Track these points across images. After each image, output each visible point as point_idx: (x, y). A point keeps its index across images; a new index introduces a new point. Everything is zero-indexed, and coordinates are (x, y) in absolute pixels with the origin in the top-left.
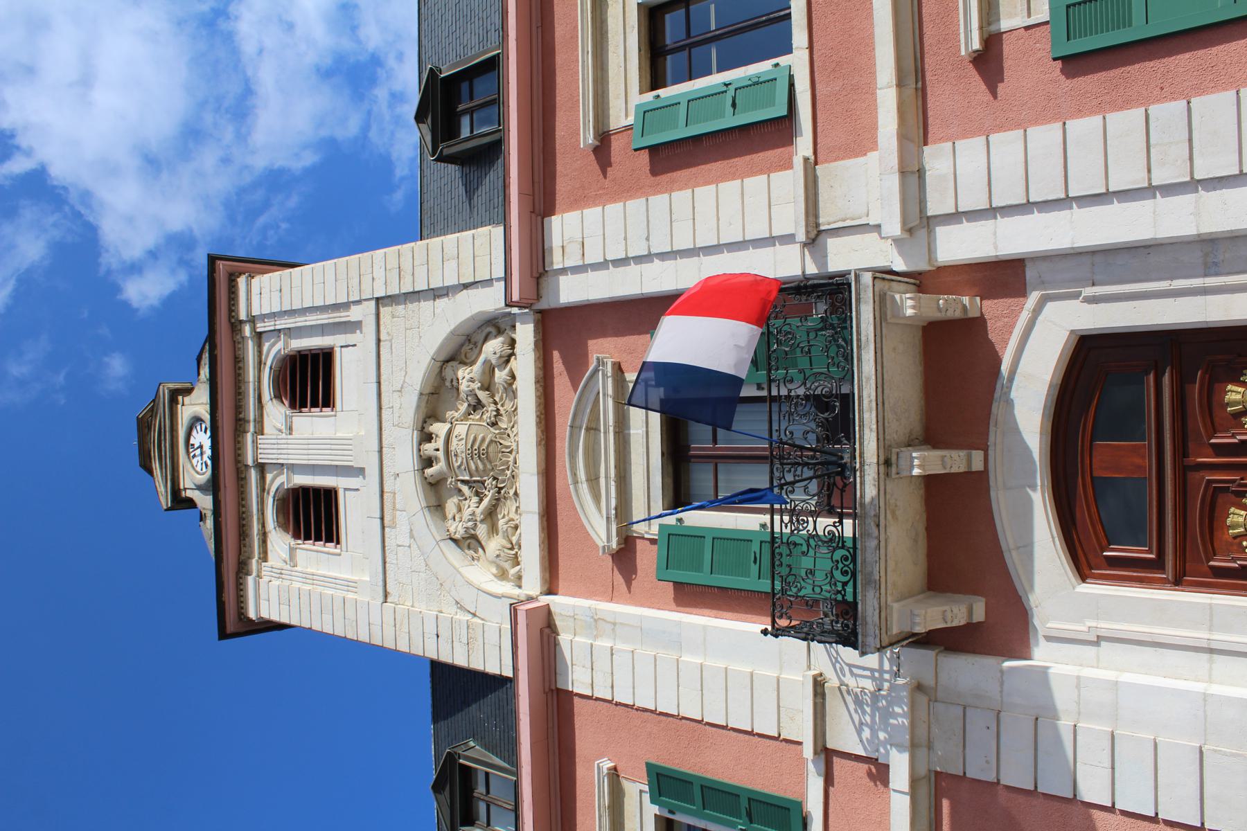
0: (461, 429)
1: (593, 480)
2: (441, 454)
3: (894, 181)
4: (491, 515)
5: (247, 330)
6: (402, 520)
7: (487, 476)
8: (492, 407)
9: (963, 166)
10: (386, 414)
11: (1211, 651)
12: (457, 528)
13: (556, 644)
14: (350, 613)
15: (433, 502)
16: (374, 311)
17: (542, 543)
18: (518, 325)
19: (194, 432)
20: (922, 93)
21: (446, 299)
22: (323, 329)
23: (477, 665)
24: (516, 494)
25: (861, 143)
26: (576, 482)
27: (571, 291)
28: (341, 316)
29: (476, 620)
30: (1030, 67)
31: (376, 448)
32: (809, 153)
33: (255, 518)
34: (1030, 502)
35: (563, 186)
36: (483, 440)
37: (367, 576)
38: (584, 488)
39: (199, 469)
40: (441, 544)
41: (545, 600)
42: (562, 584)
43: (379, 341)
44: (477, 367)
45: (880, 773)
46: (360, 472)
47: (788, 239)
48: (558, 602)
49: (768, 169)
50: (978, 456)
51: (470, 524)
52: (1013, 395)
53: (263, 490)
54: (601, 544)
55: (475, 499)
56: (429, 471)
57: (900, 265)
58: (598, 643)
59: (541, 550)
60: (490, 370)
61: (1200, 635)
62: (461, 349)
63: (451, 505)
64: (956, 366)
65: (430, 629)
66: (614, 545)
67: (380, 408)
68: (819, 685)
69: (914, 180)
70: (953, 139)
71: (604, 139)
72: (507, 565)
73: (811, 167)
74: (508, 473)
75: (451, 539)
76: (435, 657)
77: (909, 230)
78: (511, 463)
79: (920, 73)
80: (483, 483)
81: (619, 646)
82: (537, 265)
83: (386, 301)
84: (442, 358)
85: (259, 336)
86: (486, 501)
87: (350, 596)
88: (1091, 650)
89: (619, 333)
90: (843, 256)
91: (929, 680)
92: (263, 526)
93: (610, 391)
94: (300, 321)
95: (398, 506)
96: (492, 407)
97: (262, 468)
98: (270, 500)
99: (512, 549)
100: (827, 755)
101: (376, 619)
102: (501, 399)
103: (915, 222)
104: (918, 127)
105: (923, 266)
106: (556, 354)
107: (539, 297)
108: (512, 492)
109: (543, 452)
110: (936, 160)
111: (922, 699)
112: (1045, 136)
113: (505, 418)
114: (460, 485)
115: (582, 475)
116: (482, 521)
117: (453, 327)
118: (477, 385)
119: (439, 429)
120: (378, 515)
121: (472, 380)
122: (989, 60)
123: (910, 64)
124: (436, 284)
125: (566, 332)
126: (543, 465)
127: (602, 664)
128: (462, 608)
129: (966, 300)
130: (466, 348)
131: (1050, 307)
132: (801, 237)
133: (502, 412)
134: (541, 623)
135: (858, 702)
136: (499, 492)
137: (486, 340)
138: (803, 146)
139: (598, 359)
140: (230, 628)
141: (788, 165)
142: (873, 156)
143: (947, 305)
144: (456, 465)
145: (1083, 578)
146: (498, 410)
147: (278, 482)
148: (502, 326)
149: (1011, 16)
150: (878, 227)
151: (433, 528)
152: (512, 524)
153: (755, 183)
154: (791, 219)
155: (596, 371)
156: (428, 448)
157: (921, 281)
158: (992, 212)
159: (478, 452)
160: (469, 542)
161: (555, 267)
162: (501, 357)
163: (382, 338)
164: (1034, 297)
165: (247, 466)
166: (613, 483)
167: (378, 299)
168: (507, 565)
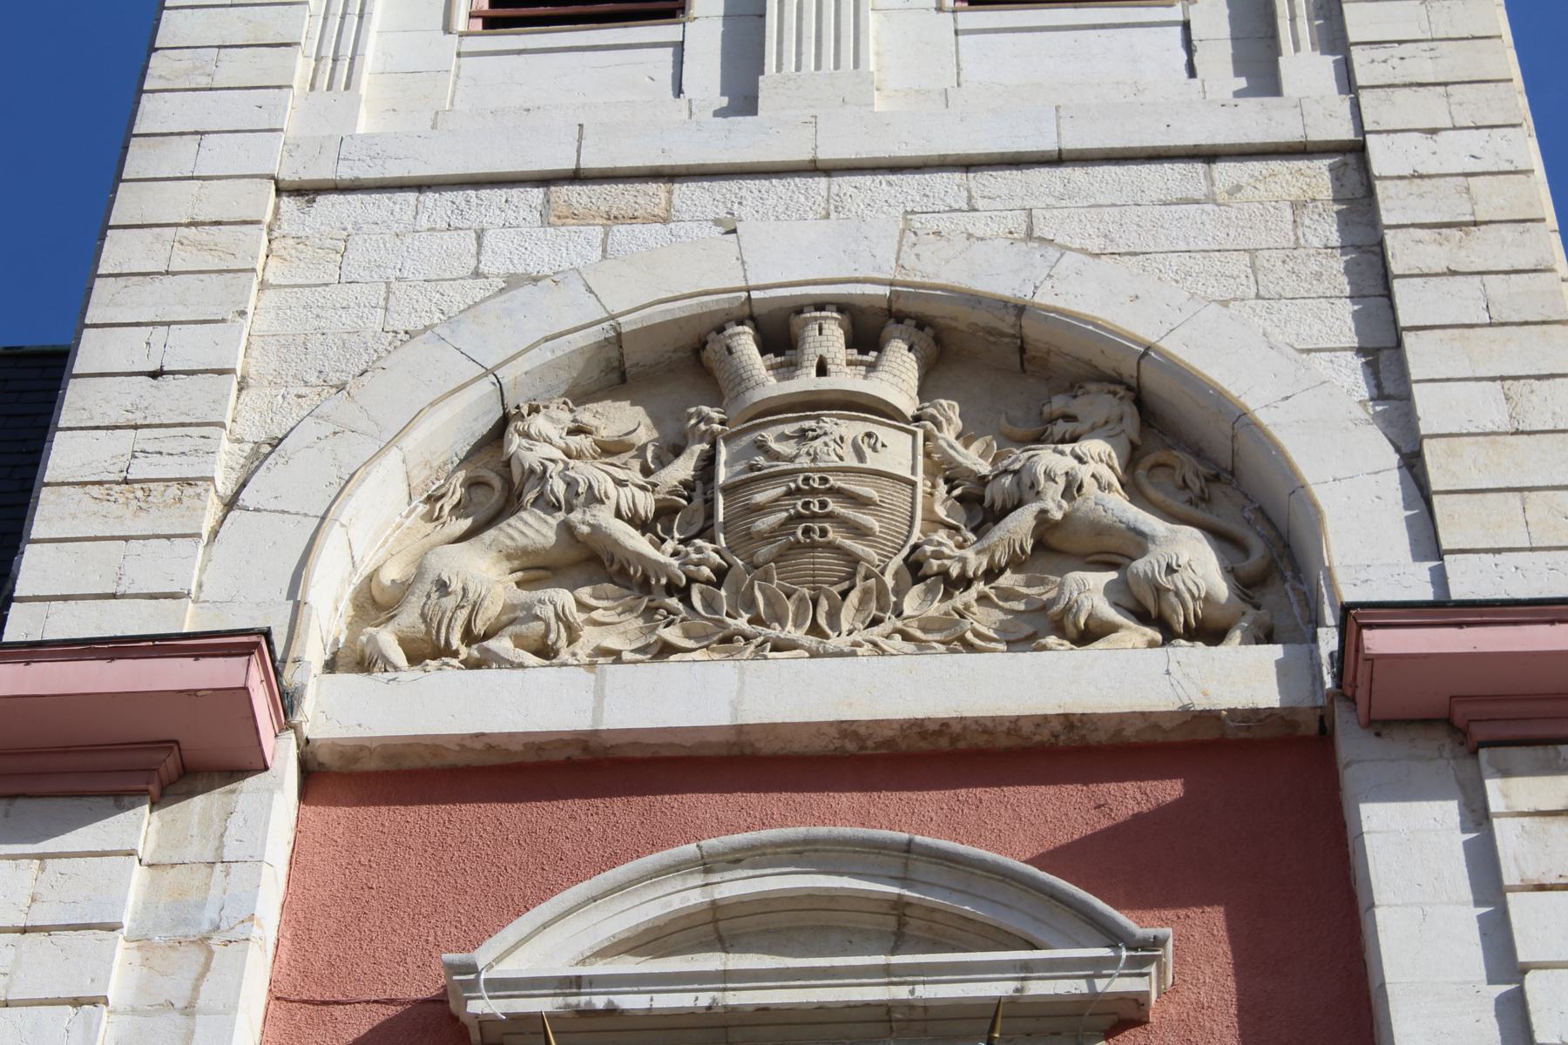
0: (896, 452)
1: (715, 927)
2: (806, 381)
4: (588, 560)
6: (575, 246)
8: (976, 562)
10: (947, 185)
12: (543, 442)
13: (120, 798)
15: (635, 356)
16: (1317, 135)
17: (488, 742)
18: (1276, 651)
21: (1364, 392)
23: (51, 514)
24: (665, 650)
26: (707, 864)
27: (1406, 845)
29: (213, 509)
36: (860, 532)
37: (375, 122)
38: (687, 895)
40: (486, 386)
41: (283, 756)
42: (338, 817)
43: (1208, 156)
44: (1119, 507)
46: (742, 97)
48: (270, 808)
51: (559, 487)
54: (482, 957)
55: (646, 504)
56: (745, 342)
58: (121, 950)
59: (464, 742)
60: (1112, 550)
62: (1189, 448)
63: (623, 418)
66: (476, 1007)
72: (409, 618)
74: (742, 623)
75: (504, 423)
78: (775, 631)
80: (706, 532)
83: (1353, 177)
84: (1152, 380)
86: (639, 543)
87: (302, 66)
93: (1039, 988)
95: (620, 232)
96: (976, 562)
99: (469, 637)
101: (218, 155)
102: (1008, 595)
106: (1170, 790)
107: (1379, 725)
108: (673, 635)
109: (818, 746)
113: (936, 608)
114: (698, 449)
115: (736, 886)
116: (567, 529)
117: (1264, 417)
118: (1054, 504)
119: (897, 376)
120: (593, 160)
121: (1072, 488)
124: (1420, 355)
126: (766, 747)
130: (1188, 466)
133: (960, 599)
136: (671, 589)
137: (1220, 537)
139: (1158, 943)
144: (769, 435)
146: (965, 582)
148: (1269, 597)
151: (545, 354)
152: (559, 636)
155: (1112, 935)
156: (829, 339)
159: (817, 509)
160: (492, 483)
161: (1493, 786)
162: (1159, 591)
166: (705, 1000)
168: (409, 618)
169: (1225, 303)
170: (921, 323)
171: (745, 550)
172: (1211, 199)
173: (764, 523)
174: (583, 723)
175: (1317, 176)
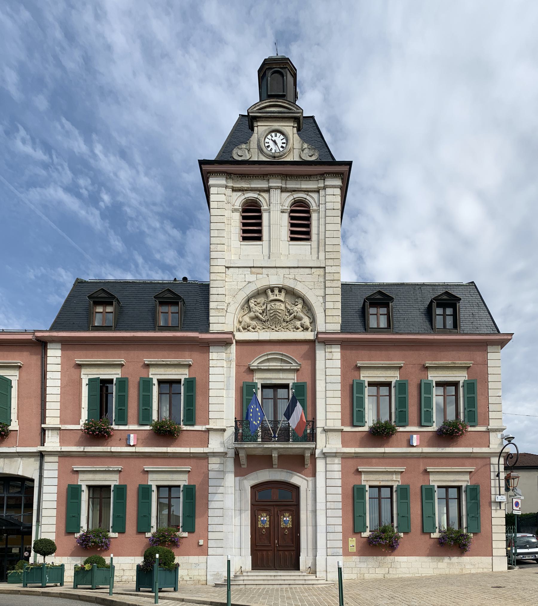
0: (282, 307)
2: (275, 298)
6: (252, 278)
9: (336, 465)
10: (287, 270)
12: (252, 305)
14: (219, 247)
15: (260, 292)
16: (321, 266)
17: (250, 340)
18: (313, 333)
25: (345, 444)
26: (267, 355)
27: (320, 354)
30: (353, 481)
32: (344, 430)
33: (249, 186)
36: (280, 316)
44: (302, 315)
53: (260, 191)
55: (261, 311)
60: (300, 319)
62: (308, 307)
65: (220, 291)
69: (334, 455)
73: (342, 431)
76: (211, 286)
77: (324, 454)
82: (327, 342)
86: (261, 316)
87: (226, 247)
92: (246, 190)
98: (256, 196)
103: (326, 455)
104: (345, 457)
105: (316, 456)
107: (319, 342)
110: (337, 460)
112: (339, 483)
118: (295, 314)
119: (282, 297)
120: (255, 266)
130: (307, 308)
132: (325, 428)
134: (228, 341)
140: (205, 167)
141: (342, 425)
142: (341, 446)
144: (272, 304)
147: (263, 199)
148: (312, 325)
153: (339, 416)
154: (331, 425)
155: (297, 363)
156: (276, 292)
157: (313, 455)
163: (313, 269)
171: (270, 320)
172: (311, 274)
174: (257, 339)
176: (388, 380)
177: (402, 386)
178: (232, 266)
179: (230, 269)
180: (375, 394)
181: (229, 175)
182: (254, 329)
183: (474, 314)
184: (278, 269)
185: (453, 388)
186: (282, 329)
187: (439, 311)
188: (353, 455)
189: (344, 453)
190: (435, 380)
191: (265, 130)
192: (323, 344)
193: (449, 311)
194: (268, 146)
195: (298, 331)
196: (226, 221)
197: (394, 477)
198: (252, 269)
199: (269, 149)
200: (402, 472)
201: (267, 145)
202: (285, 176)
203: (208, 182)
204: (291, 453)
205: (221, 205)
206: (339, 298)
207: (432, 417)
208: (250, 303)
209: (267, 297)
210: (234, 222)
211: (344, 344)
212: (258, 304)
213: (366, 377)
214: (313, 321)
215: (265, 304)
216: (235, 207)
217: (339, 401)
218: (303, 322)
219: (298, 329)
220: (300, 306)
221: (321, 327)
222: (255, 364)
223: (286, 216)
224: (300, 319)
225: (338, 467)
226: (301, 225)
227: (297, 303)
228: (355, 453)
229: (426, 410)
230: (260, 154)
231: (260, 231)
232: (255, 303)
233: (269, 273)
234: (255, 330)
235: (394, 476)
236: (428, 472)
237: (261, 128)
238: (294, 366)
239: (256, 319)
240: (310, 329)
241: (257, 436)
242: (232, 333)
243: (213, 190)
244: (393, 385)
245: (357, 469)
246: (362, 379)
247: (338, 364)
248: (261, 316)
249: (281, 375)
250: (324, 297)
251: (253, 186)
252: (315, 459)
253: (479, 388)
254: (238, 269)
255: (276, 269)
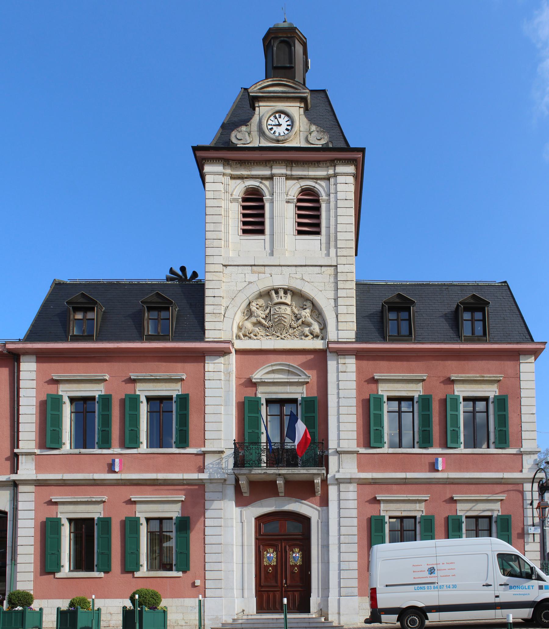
0: (288, 310)
1: (273, 372)
2: (280, 300)
3: (348, 476)
5: (331, 172)
7: (273, 325)
8: (296, 326)
9: (351, 493)
10: (294, 268)
11: (243, 546)
12: (254, 308)
14: (216, 243)
18: (322, 341)
19: (287, 119)
20: (370, 484)
21: (334, 306)
22: (328, 227)
23: (207, 318)
25: (361, 468)
26: (272, 366)
27: (332, 365)
28: (332, 244)
29: (223, 317)
30: (371, 510)
31: (281, 264)
32: (360, 452)
34: (272, 507)
35: (364, 363)
36: (285, 322)
38: (270, 369)
39: (270, 122)
40: (247, 300)
41: (233, 351)
43: (321, 266)
44: (310, 320)
45: (202, 470)
47: (339, 446)
48: (233, 356)
49: (358, 439)
50: (283, 494)
52: (297, 503)
54: (253, 376)
55: (264, 316)
56: (273, 292)
57: (329, 476)
58: (222, 374)
60: (309, 325)
61: (246, 543)
62: (317, 312)
64: (304, 489)
65: (217, 293)
66: (253, 380)
67: (296, 266)
68: (222, 452)
69: (349, 481)
70: (358, 491)
71: (376, 381)
72: (243, 331)
73: (357, 453)
75: (250, 303)
77: (337, 479)
79: (375, 483)
80: (270, 320)
81: (223, 382)
82: (341, 353)
85: (327, 178)
86: (263, 321)
87: (223, 242)
88: (239, 521)
89: (318, 382)
90: (333, 461)
91: (227, 482)
92: (246, 178)
93: (300, 380)
94: (332, 220)
97: (271, 178)
100: (204, 454)
101: (216, 260)
103: (339, 481)
104: (361, 483)
105: (328, 483)
107: (330, 352)
110: (353, 487)
111: (222, 481)
112: (354, 513)
115: (275, 368)
117: (324, 309)
118: (304, 319)
119: (288, 300)
120: (256, 264)
121: (305, 317)
122: (375, 501)
123: (377, 481)
125: (319, 359)
127: (216, 376)
128: (226, 310)
129: (320, 493)
130: (317, 313)
131: (317, 512)
135: (219, 463)
138: (362, 450)
140: (200, 154)
141: (358, 446)
142: (356, 470)
143: (318, 489)
144: (276, 308)
145: (256, 519)
149: (384, 506)
150: (338, 471)
153: (354, 435)
155: (306, 375)
156: (281, 293)
157: (325, 482)
158: (339, 500)
160: (249, 313)
163: (323, 268)
164: (319, 508)
165: (271, 168)
167: (337, 266)
168: (243, 331)
169: (321, 291)
170: (291, 291)
173: (276, 320)
174: (260, 348)
175: (331, 270)
176: (410, 394)
177: (425, 401)
178: (230, 264)
179: (228, 267)
180: (397, 409)
181: (226, 162)
182: (256, 336)
183: (506, 318)
184: (283, 268)
185: (484, 403)
186: (289, 336)
187: (467, 316)
188: (371, 481)
189: (360, 479)
190: (462, 395)
191: (268, 112)
192: (335, 354)
193: (478, 315)
194: (271, 129)
195: (307, 338)
196: (223, 214)
197: (418, 506)
198: (254, 267)
199: (272, 132)
200: (426, 500)
201: (270, 127)
202: (290, 163)
203: (203, 169)
204: (297, 478)
205: (217, 195)
206: (353, 302)
207: (460, 438)
208: (251, 306)
209: (271, 299)
210: (234, 213)
211: (360, 355)
212: (260, 307)
213: (385, 390)
214: (324, 327)
215: (269, 308)
216: (234, 197)
217: (354, 418)
218: (312, 328)
219: (307, 336)
220: (308, 311)
221: (332, 335)
222: (257, 376)
223: (292, 207)
224: (309, 325)
225: (353, 495)
226: (310, 217)
227: (305, 307)
228: (372, 479)
229: (452, 429)
230: (262, 139)
231: (262, 223)
232: (258, 306)
233: (273, 272)
234: (258, 337)
235: (418, 505)
236: (456, 500)
237: (264, 109)
238: (302, 379)
239: (258, 325)
240: (319, 338)
241: (260, 461)
242: (229, 342)
243: (208, 178)
244: (415, 400)
245: (375, 498)
246: (380, 393)
247: (353, 376)
248: (263, 321)
249: (288, 389)
250: (336, 300)
251: (254, 173)
252: (327, 486)
253: (510, 404)
254: (237, 267)
255: (280, 268)
